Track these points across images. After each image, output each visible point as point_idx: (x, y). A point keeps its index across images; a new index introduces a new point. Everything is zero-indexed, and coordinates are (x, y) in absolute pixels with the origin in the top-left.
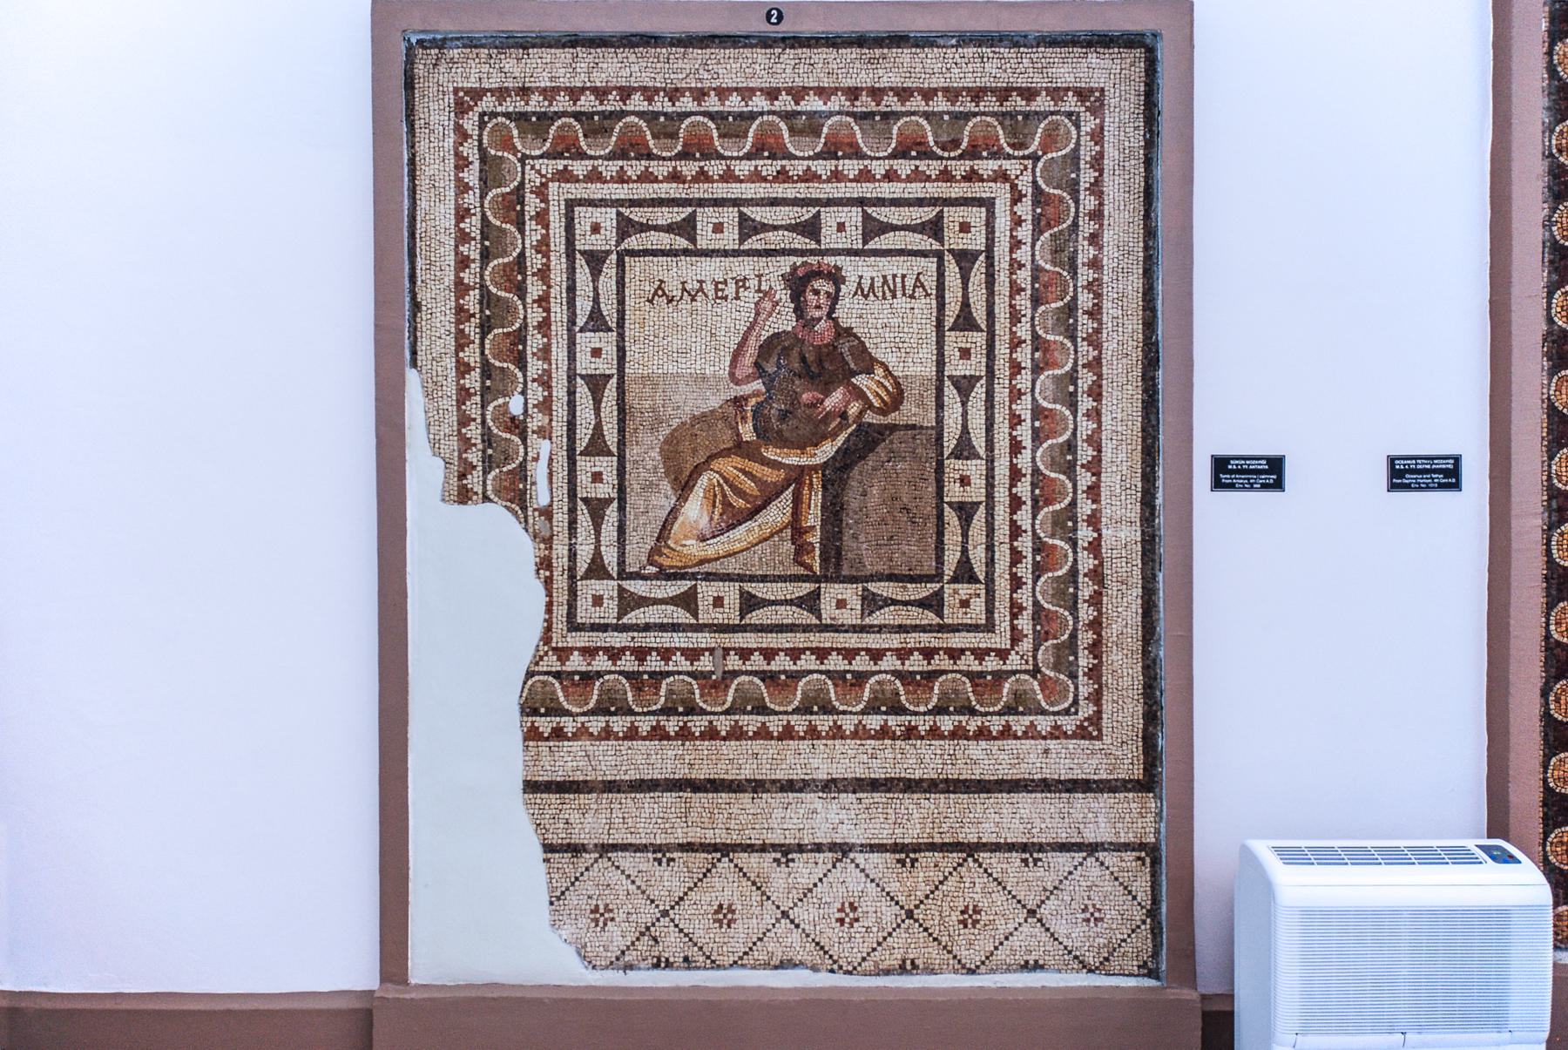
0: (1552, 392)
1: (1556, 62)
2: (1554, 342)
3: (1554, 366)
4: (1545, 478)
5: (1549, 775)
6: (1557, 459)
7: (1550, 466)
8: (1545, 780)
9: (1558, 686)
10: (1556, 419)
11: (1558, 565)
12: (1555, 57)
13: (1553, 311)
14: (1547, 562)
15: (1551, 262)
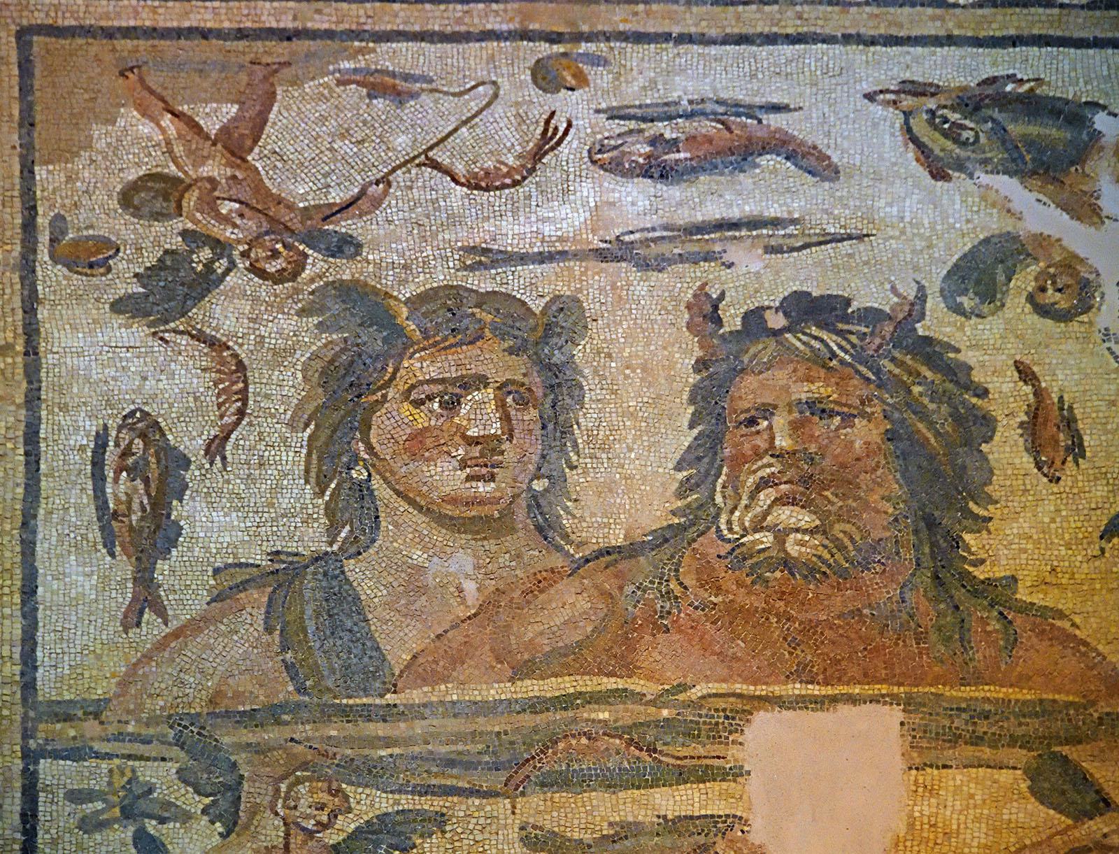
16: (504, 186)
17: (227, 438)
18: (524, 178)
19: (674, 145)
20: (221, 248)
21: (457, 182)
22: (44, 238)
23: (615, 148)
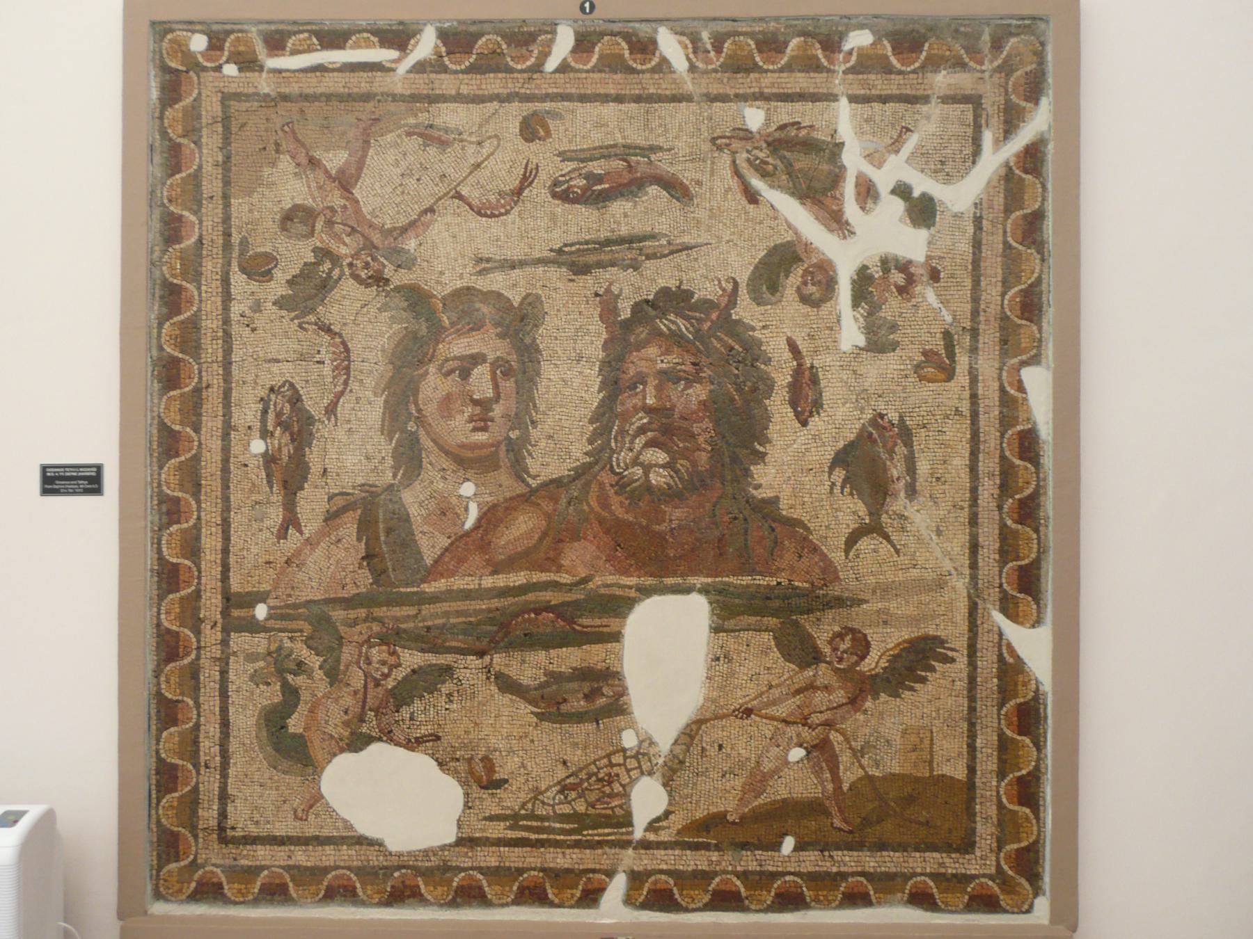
0: (162, 410)
1: (166, 125)
2: (164, 366)
3: (164, 388)
4: (155, 485)
5: (161, 747)
6: (166, 469)
7: (159, 474)
8: (157, 752)
9: (168, 668)
10: (166, 433)
11: (168, 561)
12: (166, 121)
13: (163, 340)
14: (159, 559)
15: (161, 297)
16: (501, 214)
17: (338, 401)
18: (512, 208)
19: (599, 179)
20: (335, 260)
21: (473, 210)
22: (235, 254)
23: (567, 181)
